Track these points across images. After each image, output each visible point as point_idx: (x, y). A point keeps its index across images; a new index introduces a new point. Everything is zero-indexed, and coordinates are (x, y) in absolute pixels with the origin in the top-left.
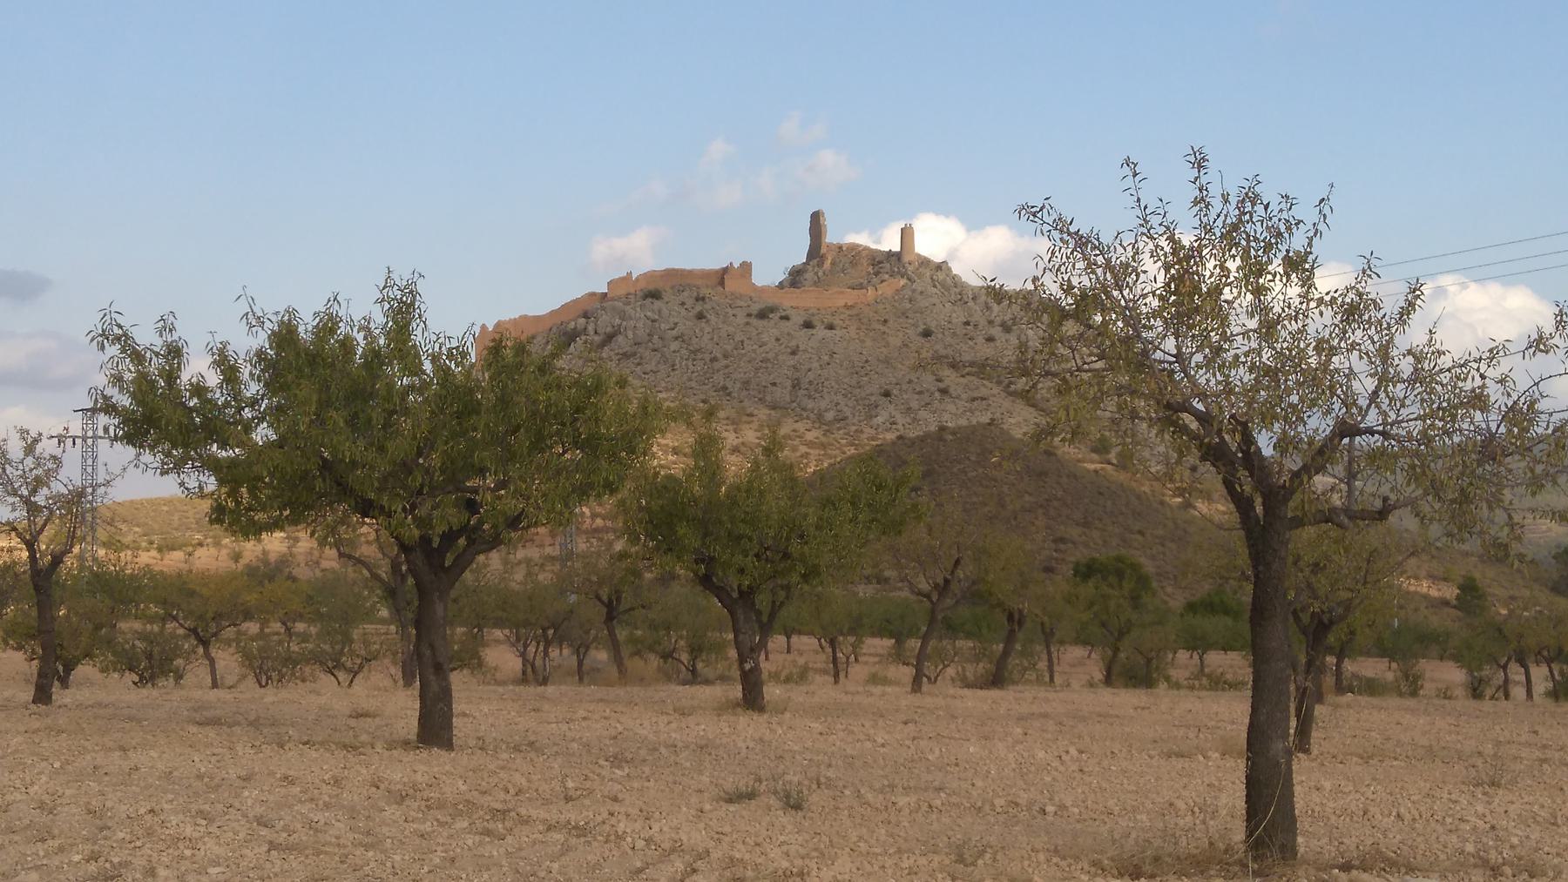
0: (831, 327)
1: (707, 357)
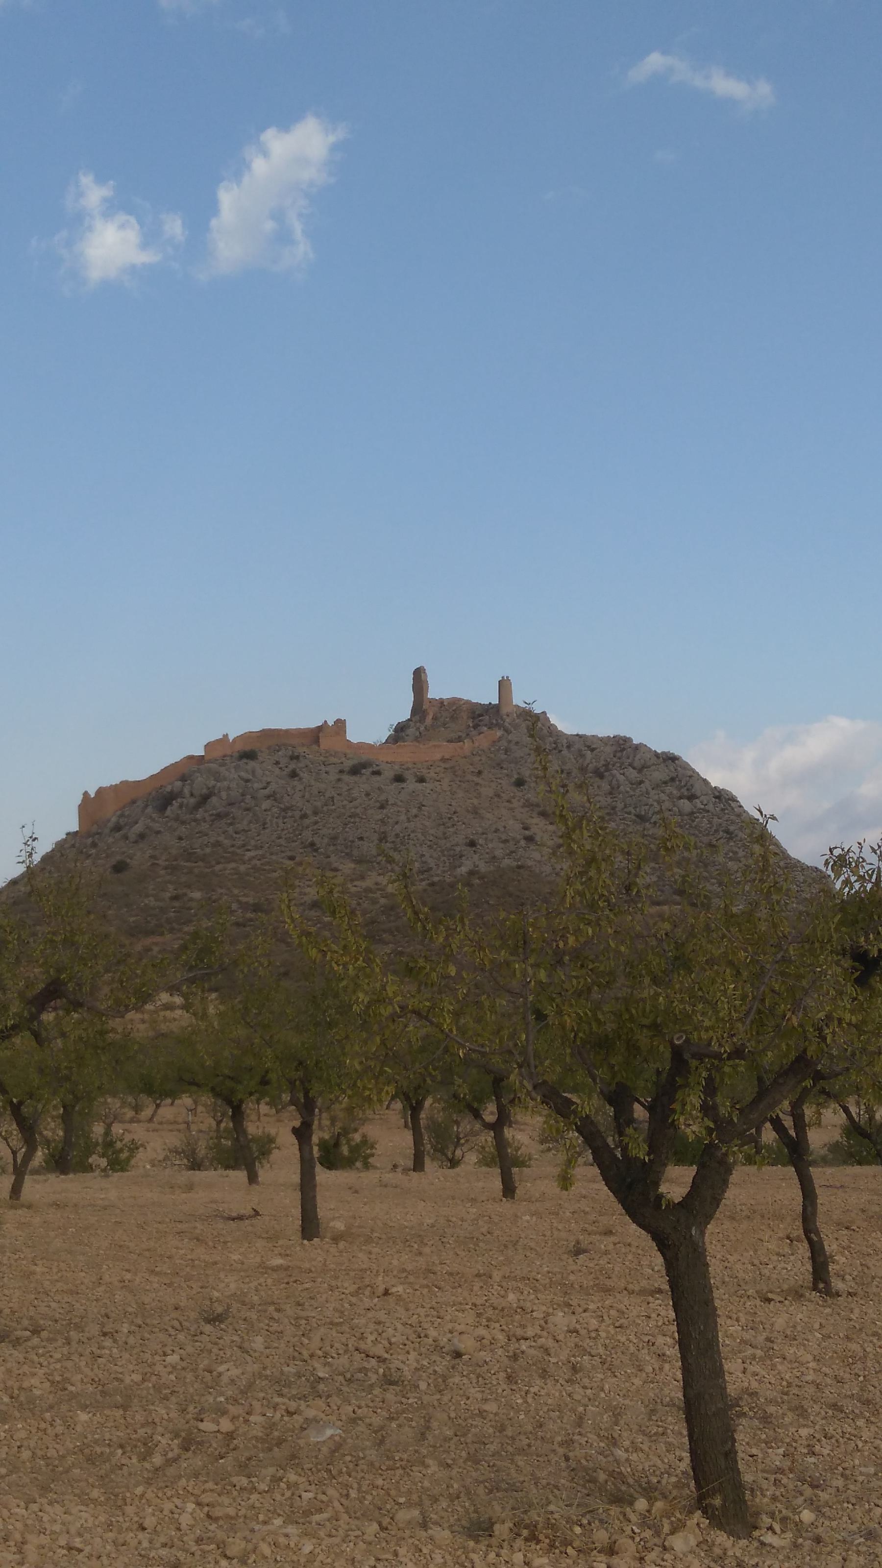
0: (421, 780)
1: (297, 814)
